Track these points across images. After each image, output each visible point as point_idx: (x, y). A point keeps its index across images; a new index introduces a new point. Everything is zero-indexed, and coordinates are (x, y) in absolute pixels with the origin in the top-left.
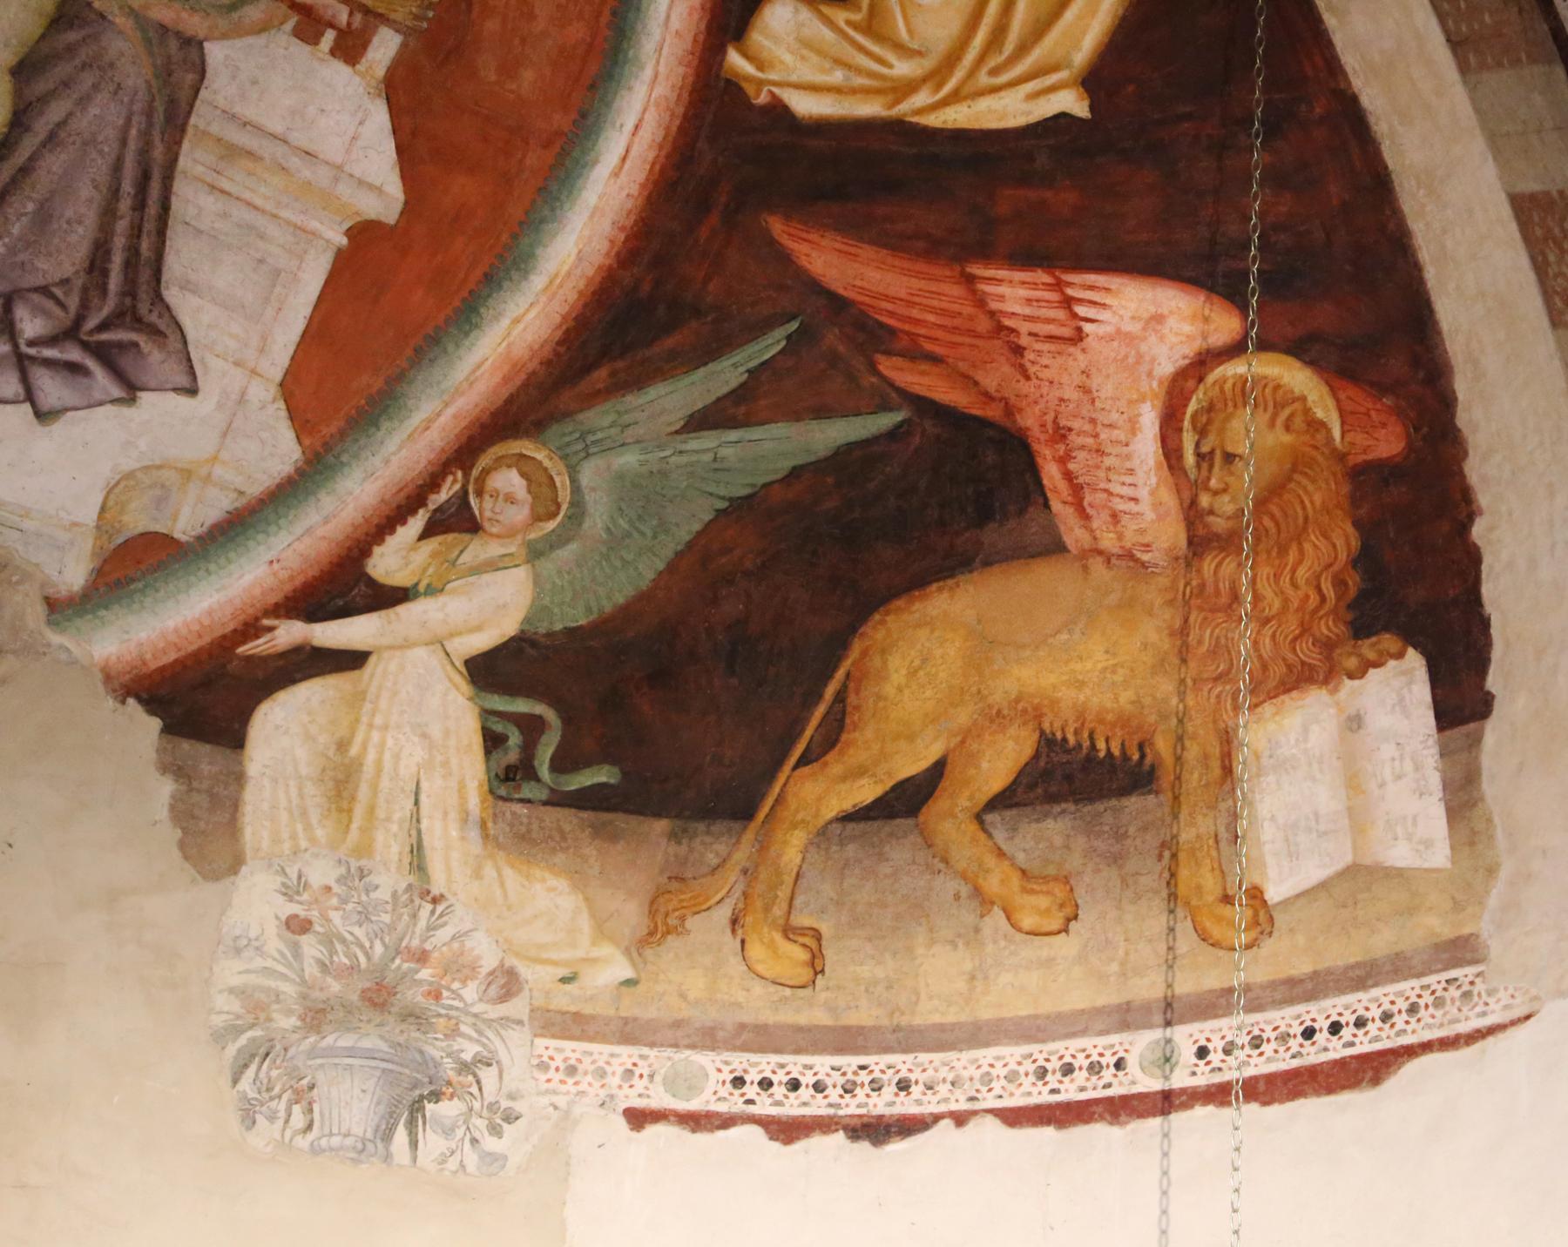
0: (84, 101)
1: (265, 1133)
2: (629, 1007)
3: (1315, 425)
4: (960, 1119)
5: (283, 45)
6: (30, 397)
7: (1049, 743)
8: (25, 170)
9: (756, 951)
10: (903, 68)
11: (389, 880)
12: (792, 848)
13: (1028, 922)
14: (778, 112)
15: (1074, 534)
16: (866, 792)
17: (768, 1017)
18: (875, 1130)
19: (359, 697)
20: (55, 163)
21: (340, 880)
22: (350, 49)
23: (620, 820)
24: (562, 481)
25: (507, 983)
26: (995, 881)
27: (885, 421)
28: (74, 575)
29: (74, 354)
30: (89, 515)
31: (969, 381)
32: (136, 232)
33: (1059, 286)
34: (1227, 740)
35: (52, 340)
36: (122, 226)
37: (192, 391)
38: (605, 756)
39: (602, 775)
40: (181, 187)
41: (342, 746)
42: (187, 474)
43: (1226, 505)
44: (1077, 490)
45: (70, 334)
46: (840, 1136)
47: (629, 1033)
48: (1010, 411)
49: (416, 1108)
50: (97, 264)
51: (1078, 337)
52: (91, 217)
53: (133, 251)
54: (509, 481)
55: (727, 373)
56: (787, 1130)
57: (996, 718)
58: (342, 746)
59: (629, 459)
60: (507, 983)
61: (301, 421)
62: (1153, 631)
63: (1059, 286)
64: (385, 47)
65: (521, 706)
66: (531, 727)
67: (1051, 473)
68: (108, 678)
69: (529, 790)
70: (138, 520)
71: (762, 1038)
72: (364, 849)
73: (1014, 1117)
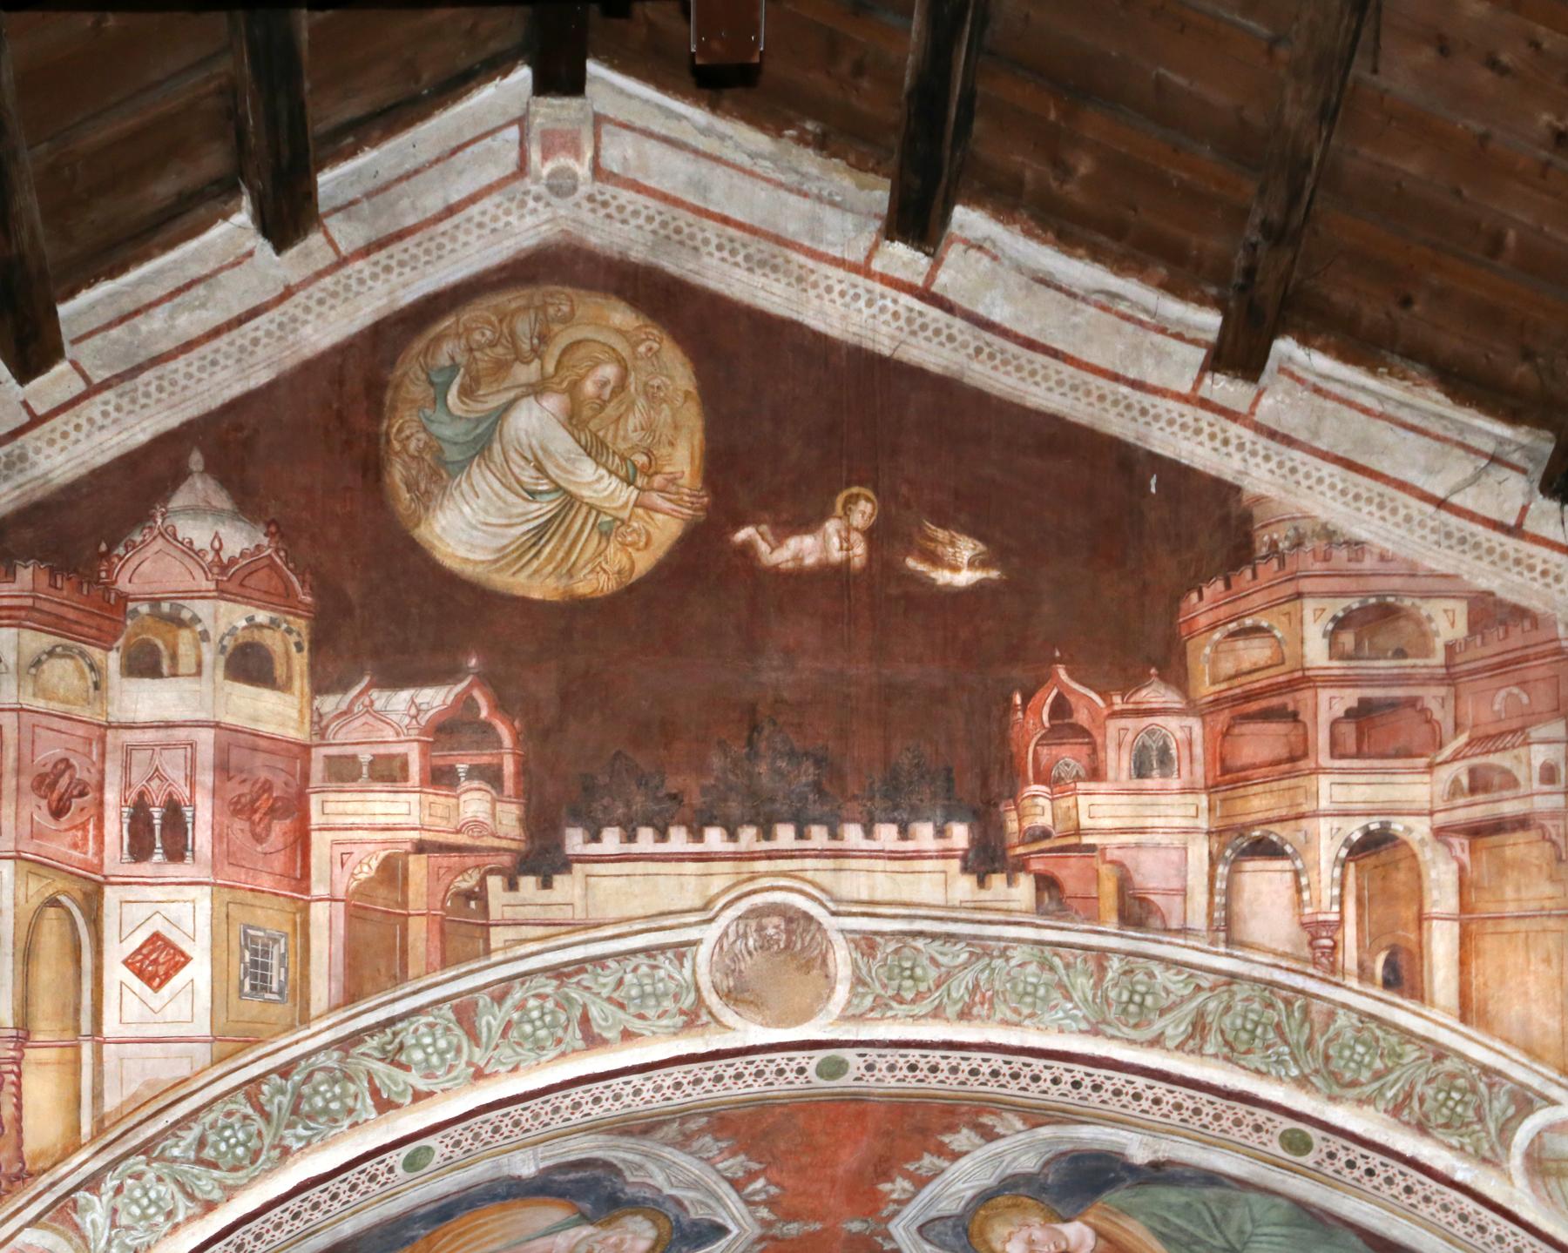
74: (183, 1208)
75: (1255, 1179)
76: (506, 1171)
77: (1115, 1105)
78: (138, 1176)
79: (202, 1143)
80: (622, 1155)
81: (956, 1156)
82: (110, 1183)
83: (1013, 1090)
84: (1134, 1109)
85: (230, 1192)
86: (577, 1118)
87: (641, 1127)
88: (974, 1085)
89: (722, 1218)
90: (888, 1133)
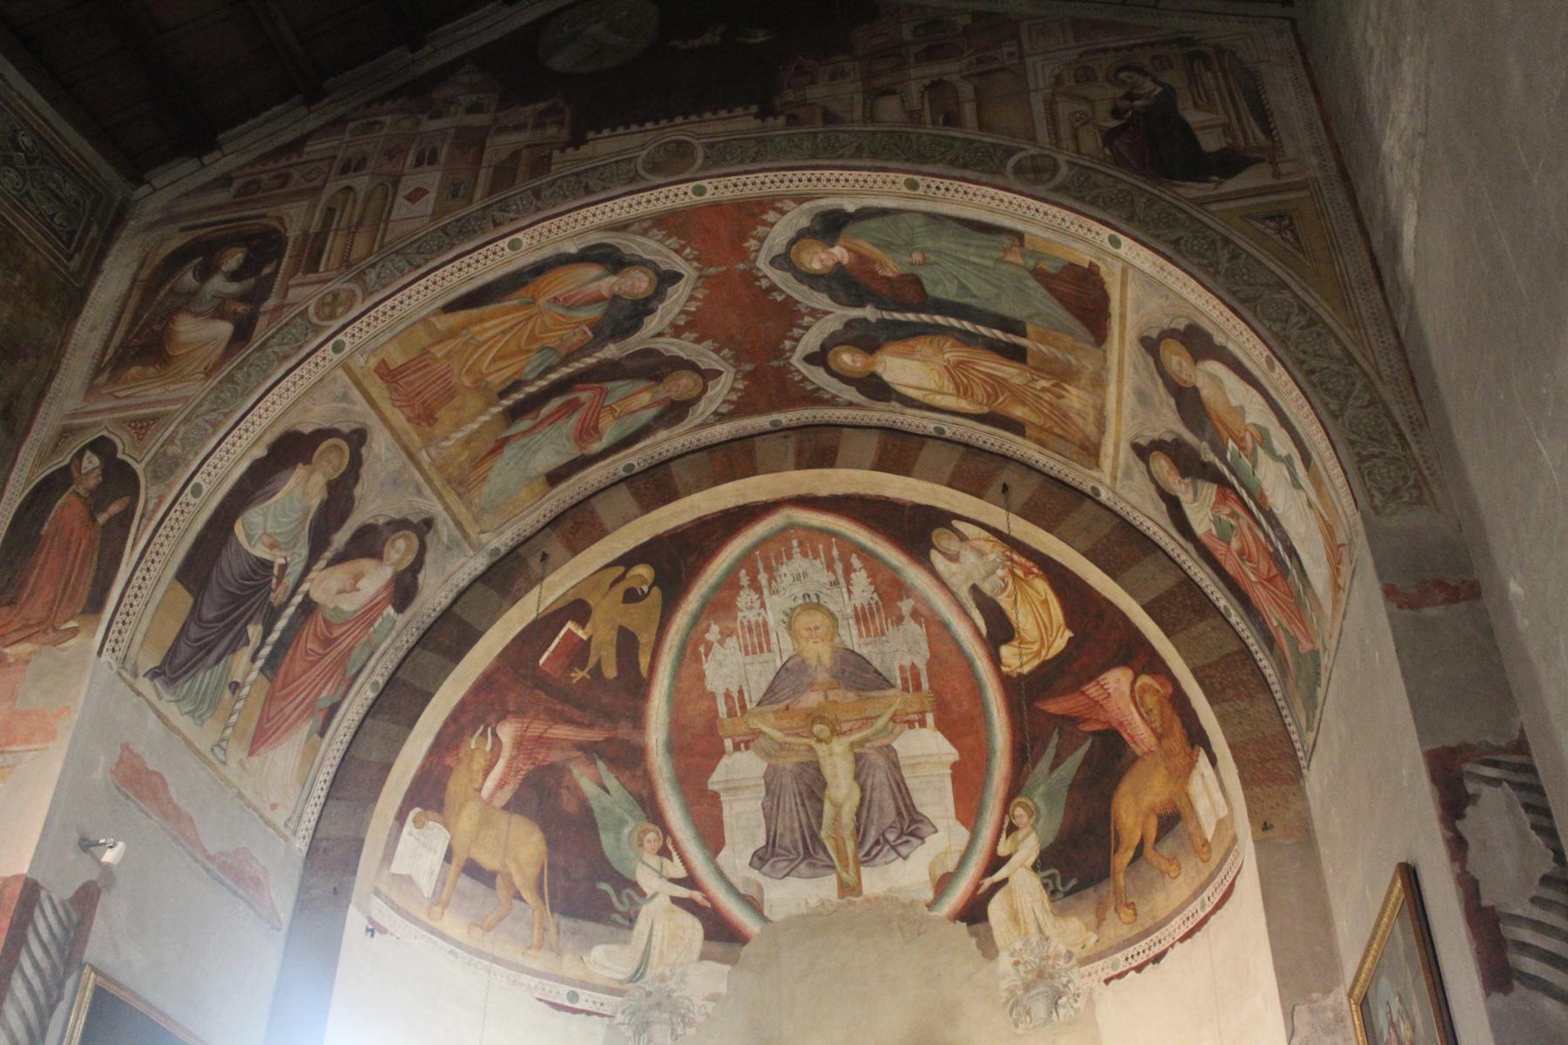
0: (874, 776)
1: (1020, 1031)
2: (1101, 948)
3: (1158, 691)
4: (1172, 946)
5: (909, 733)
6: (899, 855)
7: (1160, 817)
8: (871, 801)
9: (1122, 915)
10: (1035, 647)
11: (1035, 939)
12: (1121, 879)
13: (1173, 875)
14: (1020, 675)
15: (1138, 751)
16: (1131, 854)
17: (1129, 936)
18: (1157, 959)
19: (1010, 891)
20: (876, 795)
21: (1024, 945)
22: (923, 724)
23: (1083, 893)
24: (1030, 804)
25: (1070, 955)
26: (1163, 868)
27: (1090, 741)
28: (929, 895)
29: (905, 838)
30: (927, 878)
31: (1098, 721)
32: (904, 799)
33: (1098, 683)
34: (1187, 795)
35: (898, 838)
36: (900, 800)
37: (936, 831)
38: (1071, 878)
39: (1073, 882)
40: (907, 782)
41: (1011, 906)
42: (945, 853)
43: (1157, 724)
44: (1132, 738)
45: (902, 834)
46: (1151, 965)
47: (1101, 956)
48: (1110, 724)
49: (1056, 1003)
50: (899, 814)
51: (1109, 695)
52: (891, 801)
53: (905, 805)
54: (1019, 811)
55: (1051, 752)
56: (1139, 969)
57: (1147, 816)
58: (1011, 906)
59: (1042, 789)
60: (1070, 955)
61: (965, 823)
62: (1163, 771)
63: (1098, 683)
64: (930, 718)
65: (1048, 872)
66: (1052, 877)
67: (1125, 736)
68: (949, 918)
69: (1059, 895)
70: (939, 872)
71: (1129, 942)
72: (1027, 933)
73: (1182, 940)
74: (407, 267)
75: (902, 207)
76: (562, 251)
77: (830, 187)
78: (392, 261)
79: (420, 247)
81: (772, 225)
82: (381, 264)
83: (783, 188)
84: (839, 187)
85: (427, 261)
86: (587, 224)
87: (622, 227)
88: (765, 189)
89: (678, 269)
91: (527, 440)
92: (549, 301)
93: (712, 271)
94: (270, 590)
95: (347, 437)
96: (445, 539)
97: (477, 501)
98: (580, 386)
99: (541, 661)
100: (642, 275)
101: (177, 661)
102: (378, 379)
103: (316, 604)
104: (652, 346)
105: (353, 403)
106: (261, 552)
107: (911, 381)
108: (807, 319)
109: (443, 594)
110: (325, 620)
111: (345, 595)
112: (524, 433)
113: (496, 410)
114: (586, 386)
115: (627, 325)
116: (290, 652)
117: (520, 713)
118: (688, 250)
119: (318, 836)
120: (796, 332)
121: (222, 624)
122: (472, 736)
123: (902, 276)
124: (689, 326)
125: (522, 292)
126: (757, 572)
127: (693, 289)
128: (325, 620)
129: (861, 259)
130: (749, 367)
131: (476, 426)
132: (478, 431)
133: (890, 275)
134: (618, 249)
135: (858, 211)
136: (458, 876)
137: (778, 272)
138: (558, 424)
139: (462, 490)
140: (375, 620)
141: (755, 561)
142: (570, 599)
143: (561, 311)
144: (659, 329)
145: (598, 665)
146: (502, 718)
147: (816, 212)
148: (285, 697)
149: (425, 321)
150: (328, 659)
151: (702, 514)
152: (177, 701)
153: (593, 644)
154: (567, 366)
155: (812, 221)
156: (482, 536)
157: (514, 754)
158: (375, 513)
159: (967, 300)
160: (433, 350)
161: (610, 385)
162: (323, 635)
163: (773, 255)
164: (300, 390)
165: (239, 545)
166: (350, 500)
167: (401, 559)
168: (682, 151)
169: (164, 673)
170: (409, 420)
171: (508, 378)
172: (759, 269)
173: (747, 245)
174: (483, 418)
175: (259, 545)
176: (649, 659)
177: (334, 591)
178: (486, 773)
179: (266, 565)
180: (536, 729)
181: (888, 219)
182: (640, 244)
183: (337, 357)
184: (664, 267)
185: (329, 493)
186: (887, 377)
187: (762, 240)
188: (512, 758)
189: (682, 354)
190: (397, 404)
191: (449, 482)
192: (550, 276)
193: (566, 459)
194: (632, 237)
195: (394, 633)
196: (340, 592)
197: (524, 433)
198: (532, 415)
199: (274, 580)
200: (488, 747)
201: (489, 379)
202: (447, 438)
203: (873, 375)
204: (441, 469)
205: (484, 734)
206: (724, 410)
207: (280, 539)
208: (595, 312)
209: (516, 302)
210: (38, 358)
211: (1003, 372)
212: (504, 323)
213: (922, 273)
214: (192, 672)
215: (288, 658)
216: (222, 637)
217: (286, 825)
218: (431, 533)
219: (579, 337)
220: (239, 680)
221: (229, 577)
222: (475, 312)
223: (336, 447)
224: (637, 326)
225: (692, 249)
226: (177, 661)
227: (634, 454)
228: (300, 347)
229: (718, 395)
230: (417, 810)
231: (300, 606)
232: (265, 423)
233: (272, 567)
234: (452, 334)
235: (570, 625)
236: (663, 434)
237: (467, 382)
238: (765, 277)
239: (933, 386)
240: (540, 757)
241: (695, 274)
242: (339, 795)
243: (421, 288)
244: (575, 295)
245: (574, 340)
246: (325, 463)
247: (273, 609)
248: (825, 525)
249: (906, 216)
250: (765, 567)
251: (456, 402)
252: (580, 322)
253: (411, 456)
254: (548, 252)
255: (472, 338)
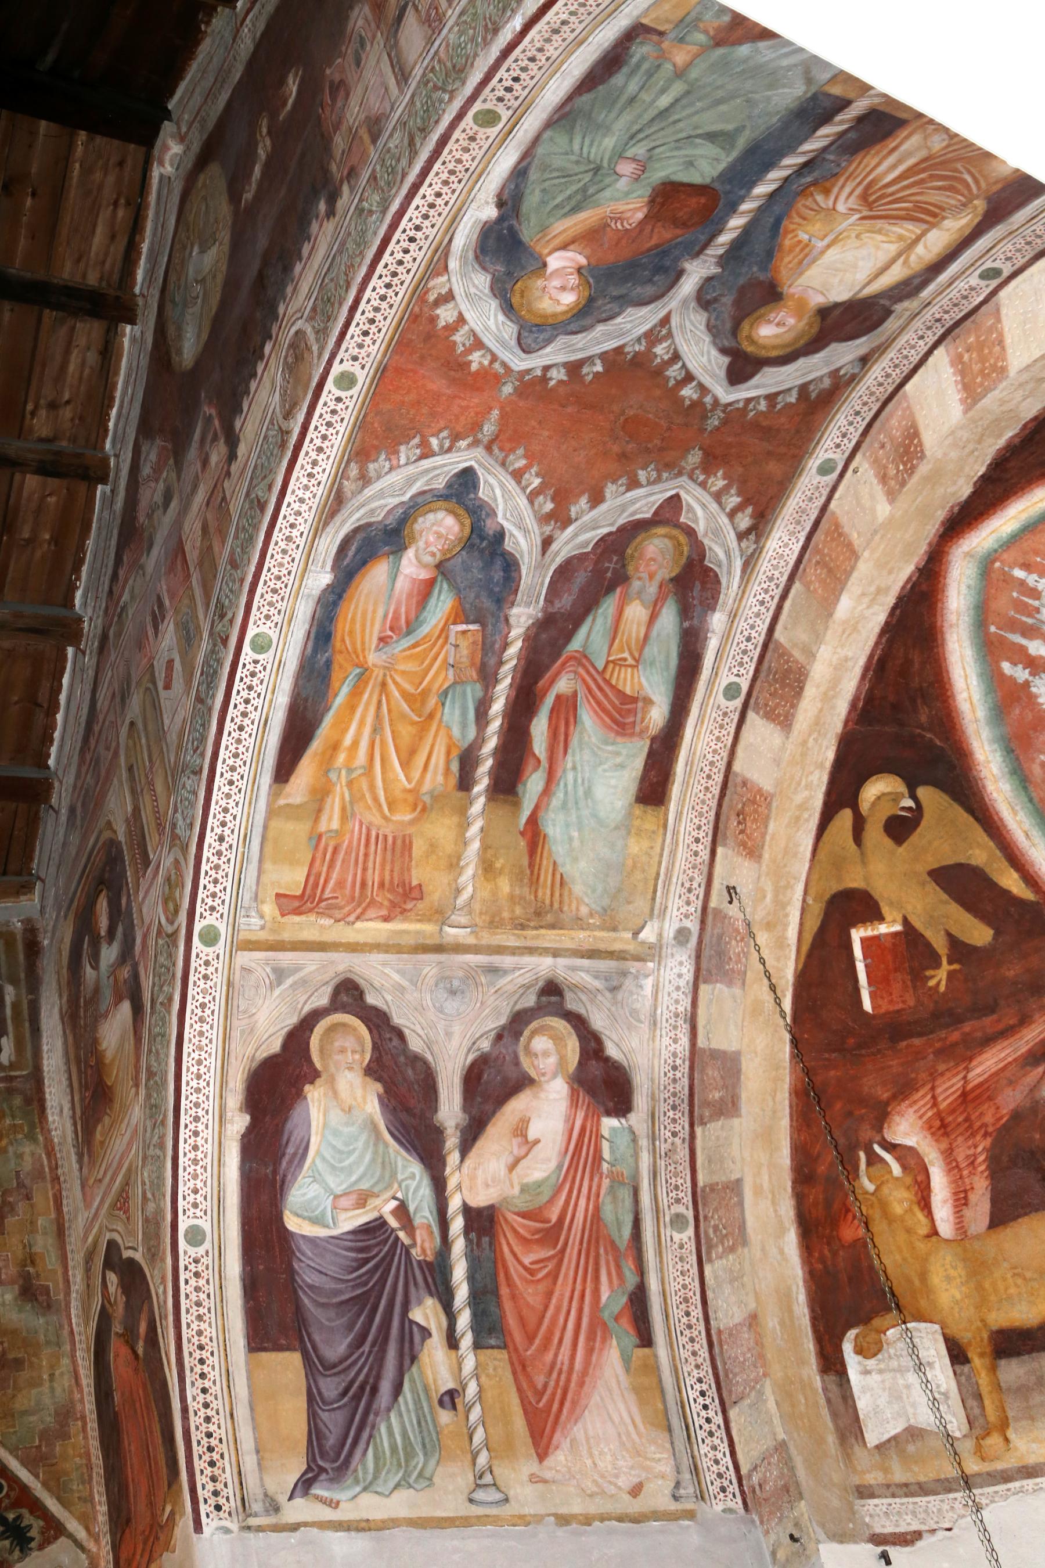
75: (523, 148)
76: (316, 593)
80: (357, 515)
90: (423, 358)
91: (560, 795)
92: (378, 649)
93: (489, 429)
94: (407, 1251)
95: (336, 1005)
96: (597, 984)
97: (584, 911)
98: (541, 683)
99: (867, 1005)
100: (431, 516)
101: (331, 1441)
102: (297, 919)
103: (492, 1207)
104: (559, 560)
105: (297, 969)
106: (351, 1221)
107: (862, 276)
108: (660, 350)
109: (666, 1041)
110: (524, 1215)
111: (523, 1163)
112: (547, 791)
113: (479, 805)
114: (548, 675)
115: (498, 575)
116: (504, 1291)
117: (904, 1090)
118: (434, 442)
119: (744, 1471)
120: (674, 372)
121: (366, 1348)
122: (857, 1176)
123: (652, 201)
124: (562, 498)
125: (336, 675)
126: (1023, 649)
127: (503, 464)
128: (524, 1215)
129: (590, 237)
130: (694, 458)
131: (476, 845)
132: (485, 847)
133: (640, 215)
134: (369, 525)
135: (500, 204)
136: (993, 1369)
137: (548, 349)
138: (574, 742)
139: (549, 918)
140: (598, 1150)
141: (1002, 640)
142: (817, 909)
143: (406, 643)
144: (538, 541)
145: (955, 944)
146: (881, 1116)
147: (471, 255)
148: (545, 1346)
149: (272, 813)
150: (572, 1252)
151: (862, 661)
152: (365, 1489)
153: (917, 924)
154: (497, 681)
155: (484, 268)
156: (642, 936)
157: (944, 1145)
158: (466, 1043)
159: (742, 143)
160: (323, 827)
161: (576, 644)
162: (538, 1231)
163: (513, 342)
164: (217, 1020)
165: (312, 1241)
166: (416, 1060)
167: (562, 1060)
168: (298, 349)
169: (322, 1470)
170: (386, 919)
171: (448, 762)
172: (528, 371)
173: (474, 367)
174: (474, 829)
175: (343, 1216)
176: (1015, 875)
177: (503, 1171)
178: (925, 1203)
179: (376, 1228)
180: (949, 1088)
181: (533, 175)
182: (381, 494)
183: (220, 948)
184: (440, 484)
185: (378, 1079)
186: (840, 294)
187: (478, 344)
188: (948, 1155)
189: (605, 531)
190: (352, 918)
191: (523, 927)
192: (342, 628)
193: (638, 764)
194: (361, 498)
195: (644, 1142)
196: (512, 1167)
197: (547, 791)
198: (531, 763)
199: (402, 1235)
200: (896, 1169)
201: (427, 787)
202: (458, 891)
203: (824, 312)
204: (494, 923)
205: (873, 1159)
206: (744, 521)
207: (365, 1185)
208: (442, 603)
209: (345, 690)
210: (28, 1197)
211: (909, 154)
212: (362, 723)
213: (659, 174)
214: (365, 1435)
215: (508, 1305)
216: (380, 1360)
217: (676, 1498)
218: (569, 996)
219: (464, 644)
220: (451, 1385)
221: (333, 1286)
222: (316, 745)
223: (332, 1028)
224: (510, 565)
225: (436, 435)
226: (331, 1441)
227: (715, 672)
228: (174, 975)
229: (711, 517)
230: (852, 1334)
231: (467, 1230)
232: (212, 1091)
233: (384, 1223)
234: (320, 794)
235: (857, 935)
236: (717, 620)
237: (405, 816)
238: (546, 368)
239: (893, 248)
240: (988, 1119)
241: (479, 452)
242: (734, 1398)
243: (226, 789)
244: (396, 612)
245: (465, 652)
246: (339, 1057)
247: (429, 1264)
248: (1024, 516)
249: (540, 150)
250: (1024, 635)
251: (419, 848)
252: (445, 629)
253: (439, 949)
254: (304, 611)
255: (350, 770)
